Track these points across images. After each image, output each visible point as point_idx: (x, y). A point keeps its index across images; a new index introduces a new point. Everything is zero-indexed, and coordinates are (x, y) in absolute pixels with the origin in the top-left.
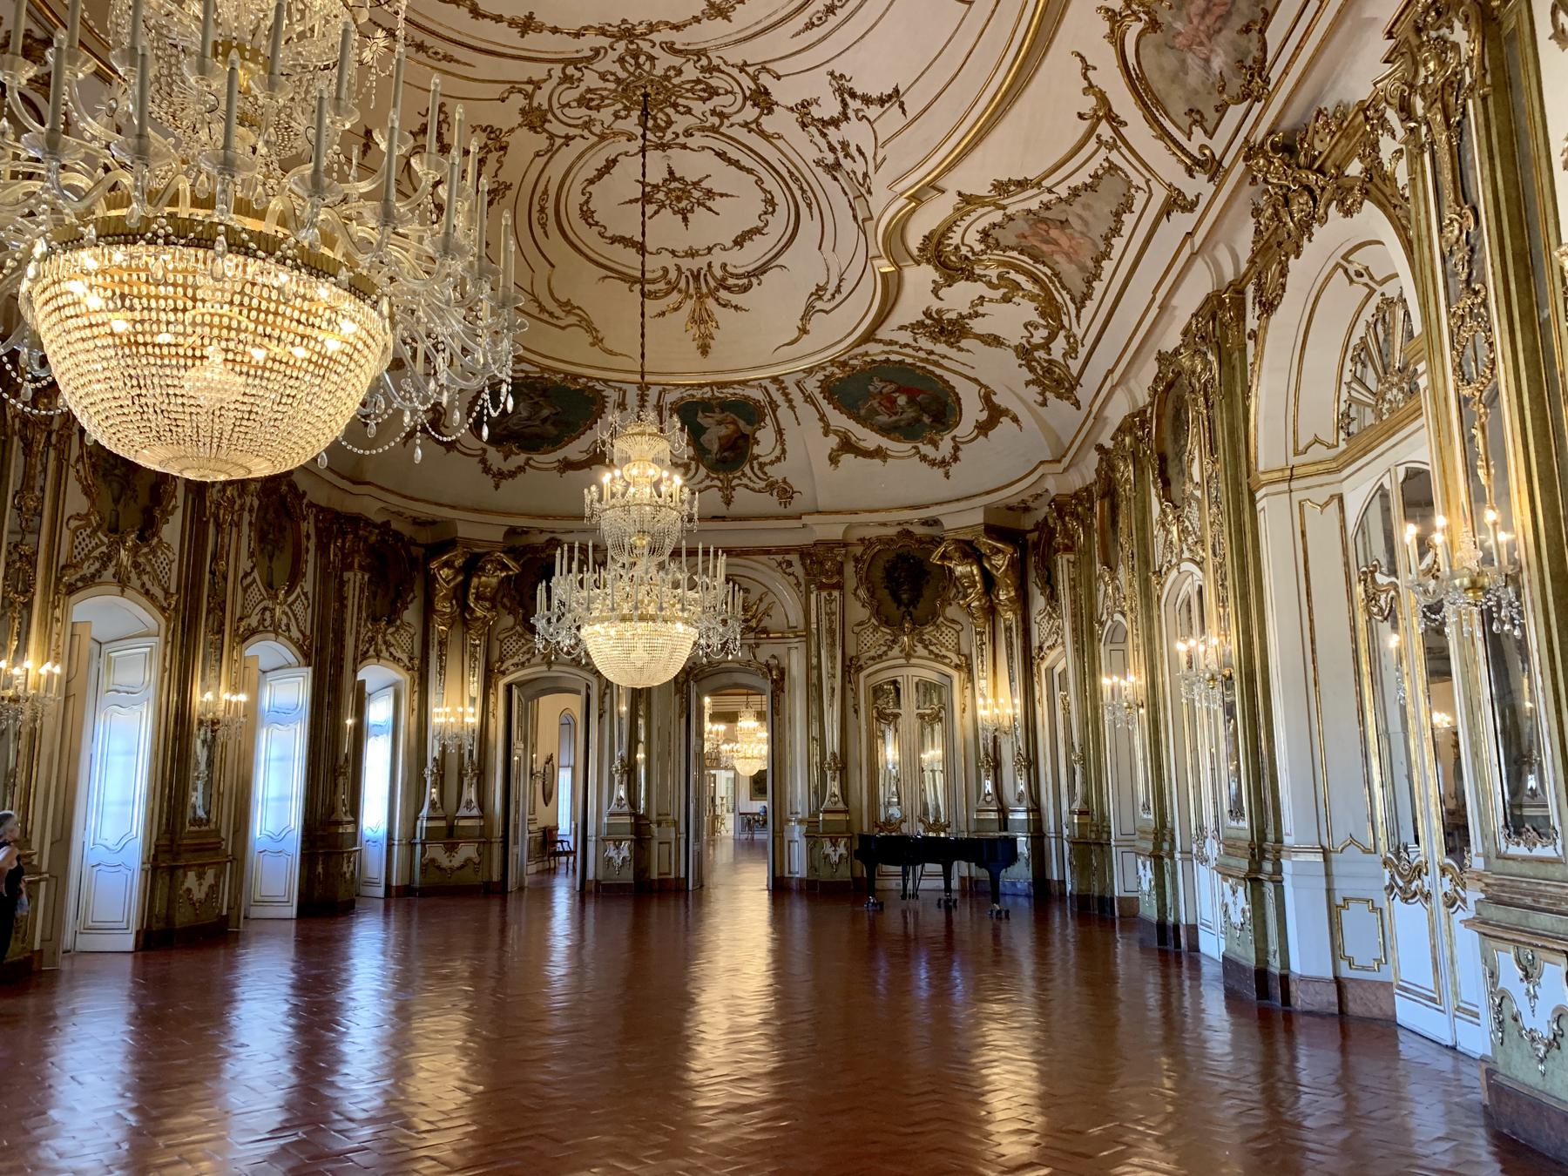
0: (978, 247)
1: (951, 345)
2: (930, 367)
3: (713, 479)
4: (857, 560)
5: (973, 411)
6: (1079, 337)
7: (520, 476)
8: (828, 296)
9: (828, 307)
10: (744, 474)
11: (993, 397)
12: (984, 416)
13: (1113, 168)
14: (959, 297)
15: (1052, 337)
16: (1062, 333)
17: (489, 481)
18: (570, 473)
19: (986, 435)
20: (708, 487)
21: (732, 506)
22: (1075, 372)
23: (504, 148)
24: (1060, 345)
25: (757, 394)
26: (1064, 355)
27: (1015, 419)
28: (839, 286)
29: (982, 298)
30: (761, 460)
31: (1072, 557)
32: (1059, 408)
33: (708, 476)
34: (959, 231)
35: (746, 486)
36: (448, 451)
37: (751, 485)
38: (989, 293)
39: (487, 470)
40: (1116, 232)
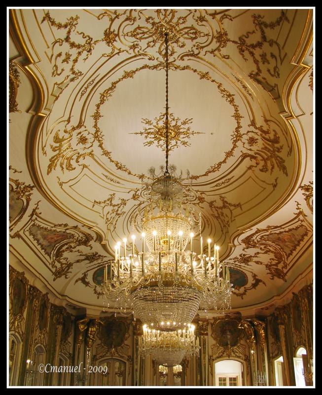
0: (259, 240)
1: (246, 264)
4: (212, 325)
5: (251, 281)
6: (288, 263)
11: (257, 277)
12: (254, 282)
13: (302, 226)
14: (251, 252)
15: (279, 263)
16: (282, 262)
17: (96, 296)
19: (255, 288)
22: (285, 272)
23: (125, 204)
24: (280, 266)
26: (282, 268)
27: (264, 283)
29: (258, 253)
31: (284, 327)
32: (279, 281)
34: (255, 236)
36: (86, 286)
38: (260, 251)
39: (96, 292)
40: (302, 240)
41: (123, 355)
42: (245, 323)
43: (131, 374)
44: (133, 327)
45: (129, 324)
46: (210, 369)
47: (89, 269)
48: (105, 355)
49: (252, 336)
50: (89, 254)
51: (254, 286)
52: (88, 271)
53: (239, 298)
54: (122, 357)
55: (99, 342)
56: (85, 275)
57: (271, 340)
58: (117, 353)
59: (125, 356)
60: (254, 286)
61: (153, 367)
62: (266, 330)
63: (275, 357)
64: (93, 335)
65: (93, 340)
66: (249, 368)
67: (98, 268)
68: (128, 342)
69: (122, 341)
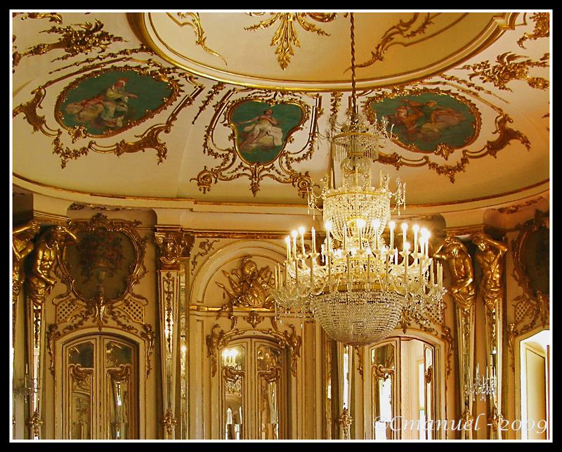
2: (468, 97)
3: (246, 168)
7: (83, 156)
8: (408, 32)
9: (407, 41)
10: (272, 167)
17: (58, 158)
18: (125, 155)
20: (238, 175)
21: (258, 193)
25: (310, 102)
28: (424, 26)
30: (290, 156)
33: (241, 166)
35: (272, 176)
36: (36, 129)
37: (277, 176)
39: (57, 150)
41: (131, 324)
42: (454, 245)
43: (152, 372)
44: (157, 246)
45: (144, 240)
46: (357, 358)
47: (52, 78)
48: (80, 323)
49: (466, 278)
50: (77, 29)
51: (493, 148)
52: (50, 83)
53: (444, 178)
54: (129, 329)
55: (62, 288)
56: (39, 97)
57: (515, 289)
58: (114, 319)
59: (136, 326)
60: (493, 148)
61: (210, 353)
62: (502, 262)
63: (522, 334)
64: (49, 270)
65: (48, 284)
66: (452, 359)
67: (80, 75)
68: (142, 287)
69: (126, 285)
